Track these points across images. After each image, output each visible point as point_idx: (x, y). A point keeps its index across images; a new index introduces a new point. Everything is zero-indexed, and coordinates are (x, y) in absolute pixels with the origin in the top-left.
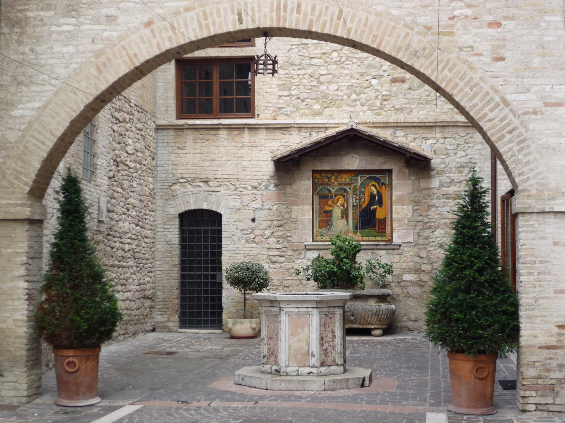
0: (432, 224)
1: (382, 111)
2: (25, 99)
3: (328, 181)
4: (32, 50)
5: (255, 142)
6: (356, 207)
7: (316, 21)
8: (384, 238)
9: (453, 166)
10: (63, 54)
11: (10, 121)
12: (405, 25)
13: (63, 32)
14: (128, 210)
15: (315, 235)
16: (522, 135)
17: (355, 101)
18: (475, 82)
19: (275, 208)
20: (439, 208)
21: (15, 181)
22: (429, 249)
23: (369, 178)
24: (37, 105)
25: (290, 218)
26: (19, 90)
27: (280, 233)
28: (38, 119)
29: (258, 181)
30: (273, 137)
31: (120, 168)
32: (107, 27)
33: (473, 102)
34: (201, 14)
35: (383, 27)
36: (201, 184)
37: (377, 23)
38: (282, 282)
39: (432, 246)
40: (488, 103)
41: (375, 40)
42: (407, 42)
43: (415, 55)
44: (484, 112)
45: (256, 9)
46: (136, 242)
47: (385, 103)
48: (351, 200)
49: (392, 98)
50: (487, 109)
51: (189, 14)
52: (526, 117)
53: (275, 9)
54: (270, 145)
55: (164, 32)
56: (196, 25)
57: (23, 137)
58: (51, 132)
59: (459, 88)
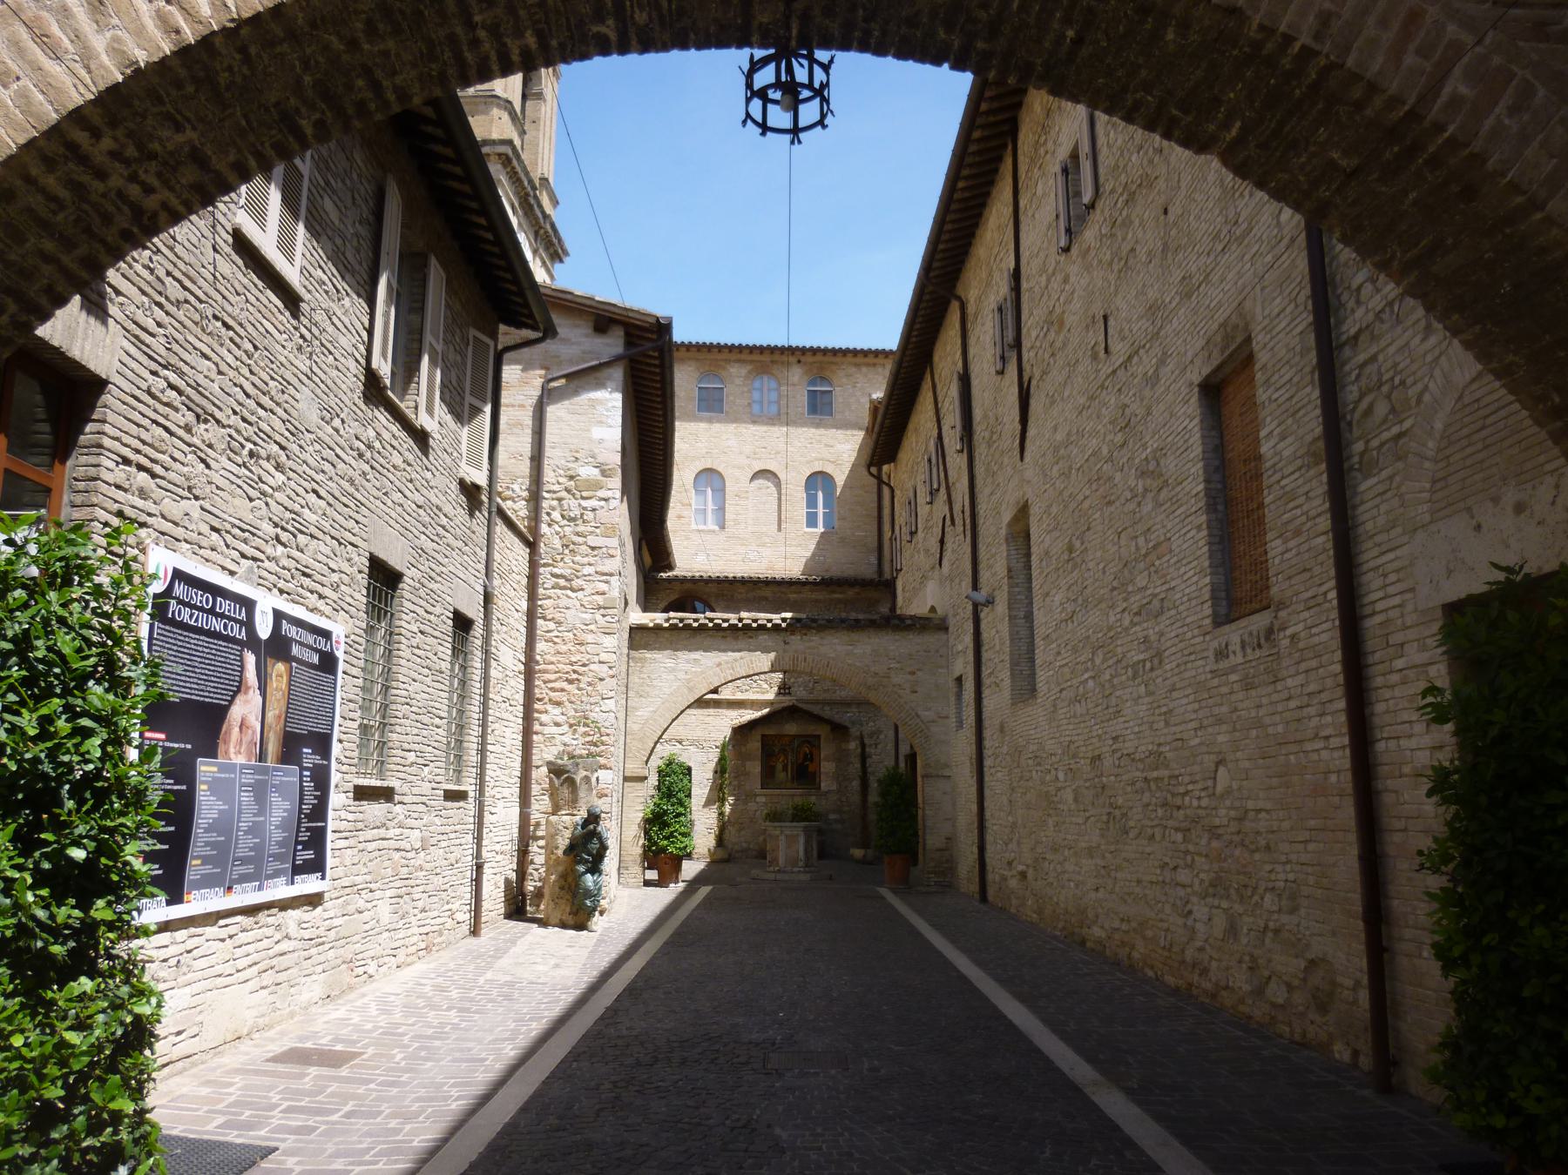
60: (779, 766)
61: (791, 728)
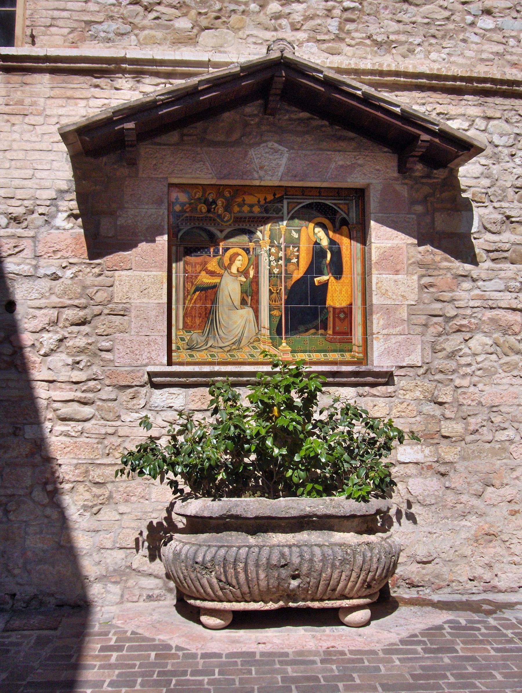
0: (465, 322)
1: (343, 46)
3: (209, 211)
5: (21, 102)
6: (278, 276)
8: (347, 356)
9: (509, 184)
15: (174, 347)
17: (277, 16)
20: (480, 283)
22: (458, 382)
23: (309, 206)
25: (110, 302)
27: (81, 342)
29: (26, 203)
30: (69, 93)
38: (87, 471)
39: (465, 375)
47: (349, 26)
49: (366, 18)
54: (61, 111)
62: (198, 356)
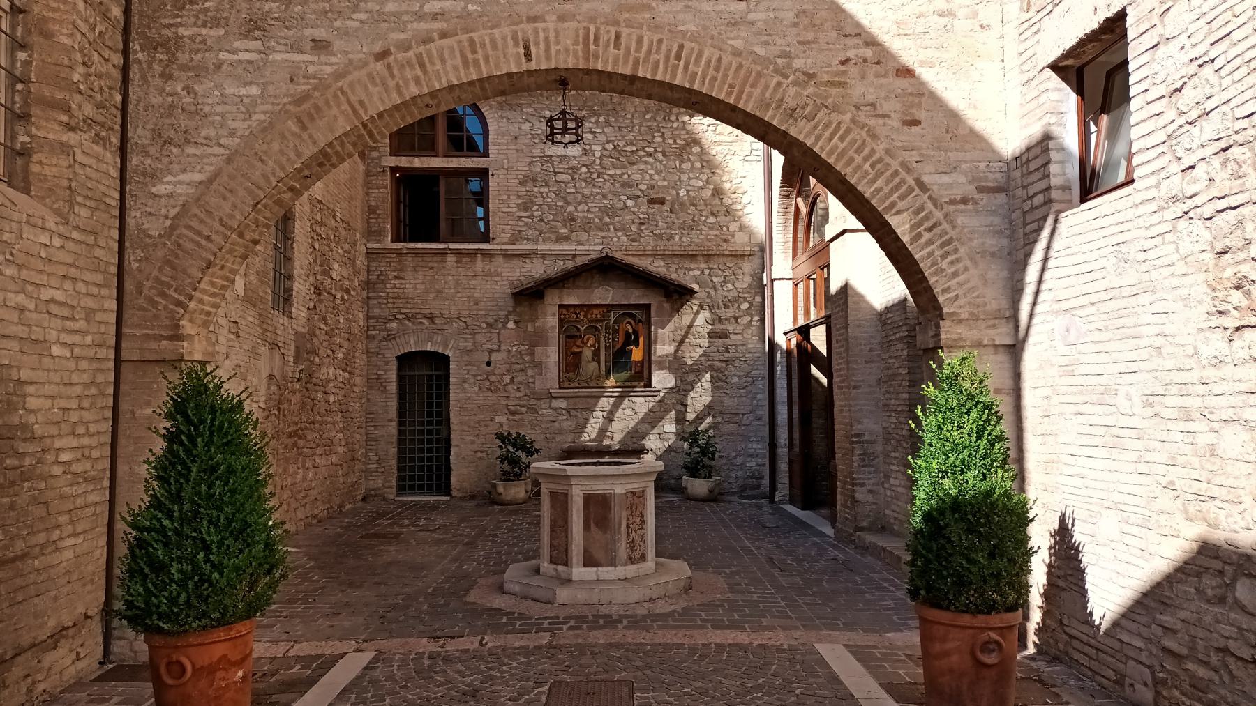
2: (176, 167)
4: (187, 89)
7: (644, 62)
10: (240, 96)
11: (150, 202)
12: (776, 71)
13: (240, 62)
14: (333, 351)
16: (947, 233)
18: (877, 156)
19: (514, 349)
21: (159, 299)
24: (198, 177)
26: (165, 154)
28: (198, 200)
31: (322, 297)
32: (315, 58)
33: (876, 185)
34: (466, 44)
35: (743, 72)
36: (424, 321)
37: (734, 66)
40: (897, 187)
41: (732, 92)
42: (779, 96)
43: (791, 116)
44: (891, 199)
45: (552, 38)
46: (343, 392)
47: (643, 227)
48: (603, 339)
50: (896, 195)
51: (445, 42)
52: (952, 208)
53: (581, 40)
55: (408, 69)
56: (459, 61)
57: (173, 228)
58: (221, 220)
59: (854, 165)
60: (587, 353)
61: (604, 294)
62: (573, 384)
